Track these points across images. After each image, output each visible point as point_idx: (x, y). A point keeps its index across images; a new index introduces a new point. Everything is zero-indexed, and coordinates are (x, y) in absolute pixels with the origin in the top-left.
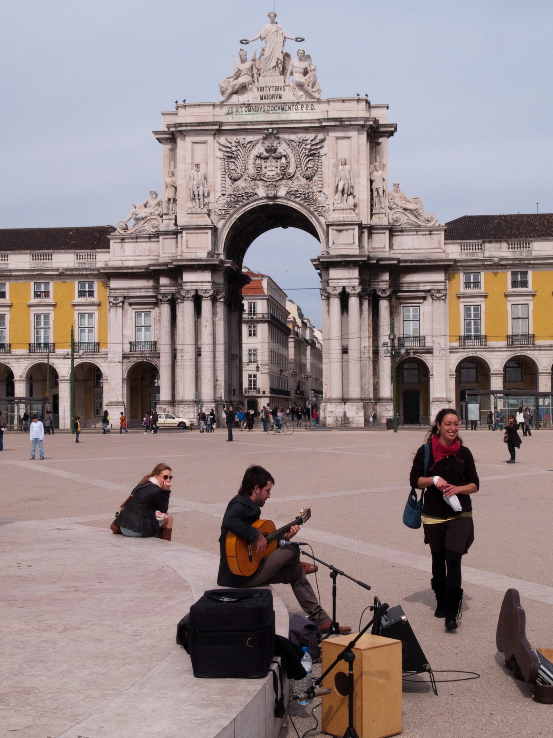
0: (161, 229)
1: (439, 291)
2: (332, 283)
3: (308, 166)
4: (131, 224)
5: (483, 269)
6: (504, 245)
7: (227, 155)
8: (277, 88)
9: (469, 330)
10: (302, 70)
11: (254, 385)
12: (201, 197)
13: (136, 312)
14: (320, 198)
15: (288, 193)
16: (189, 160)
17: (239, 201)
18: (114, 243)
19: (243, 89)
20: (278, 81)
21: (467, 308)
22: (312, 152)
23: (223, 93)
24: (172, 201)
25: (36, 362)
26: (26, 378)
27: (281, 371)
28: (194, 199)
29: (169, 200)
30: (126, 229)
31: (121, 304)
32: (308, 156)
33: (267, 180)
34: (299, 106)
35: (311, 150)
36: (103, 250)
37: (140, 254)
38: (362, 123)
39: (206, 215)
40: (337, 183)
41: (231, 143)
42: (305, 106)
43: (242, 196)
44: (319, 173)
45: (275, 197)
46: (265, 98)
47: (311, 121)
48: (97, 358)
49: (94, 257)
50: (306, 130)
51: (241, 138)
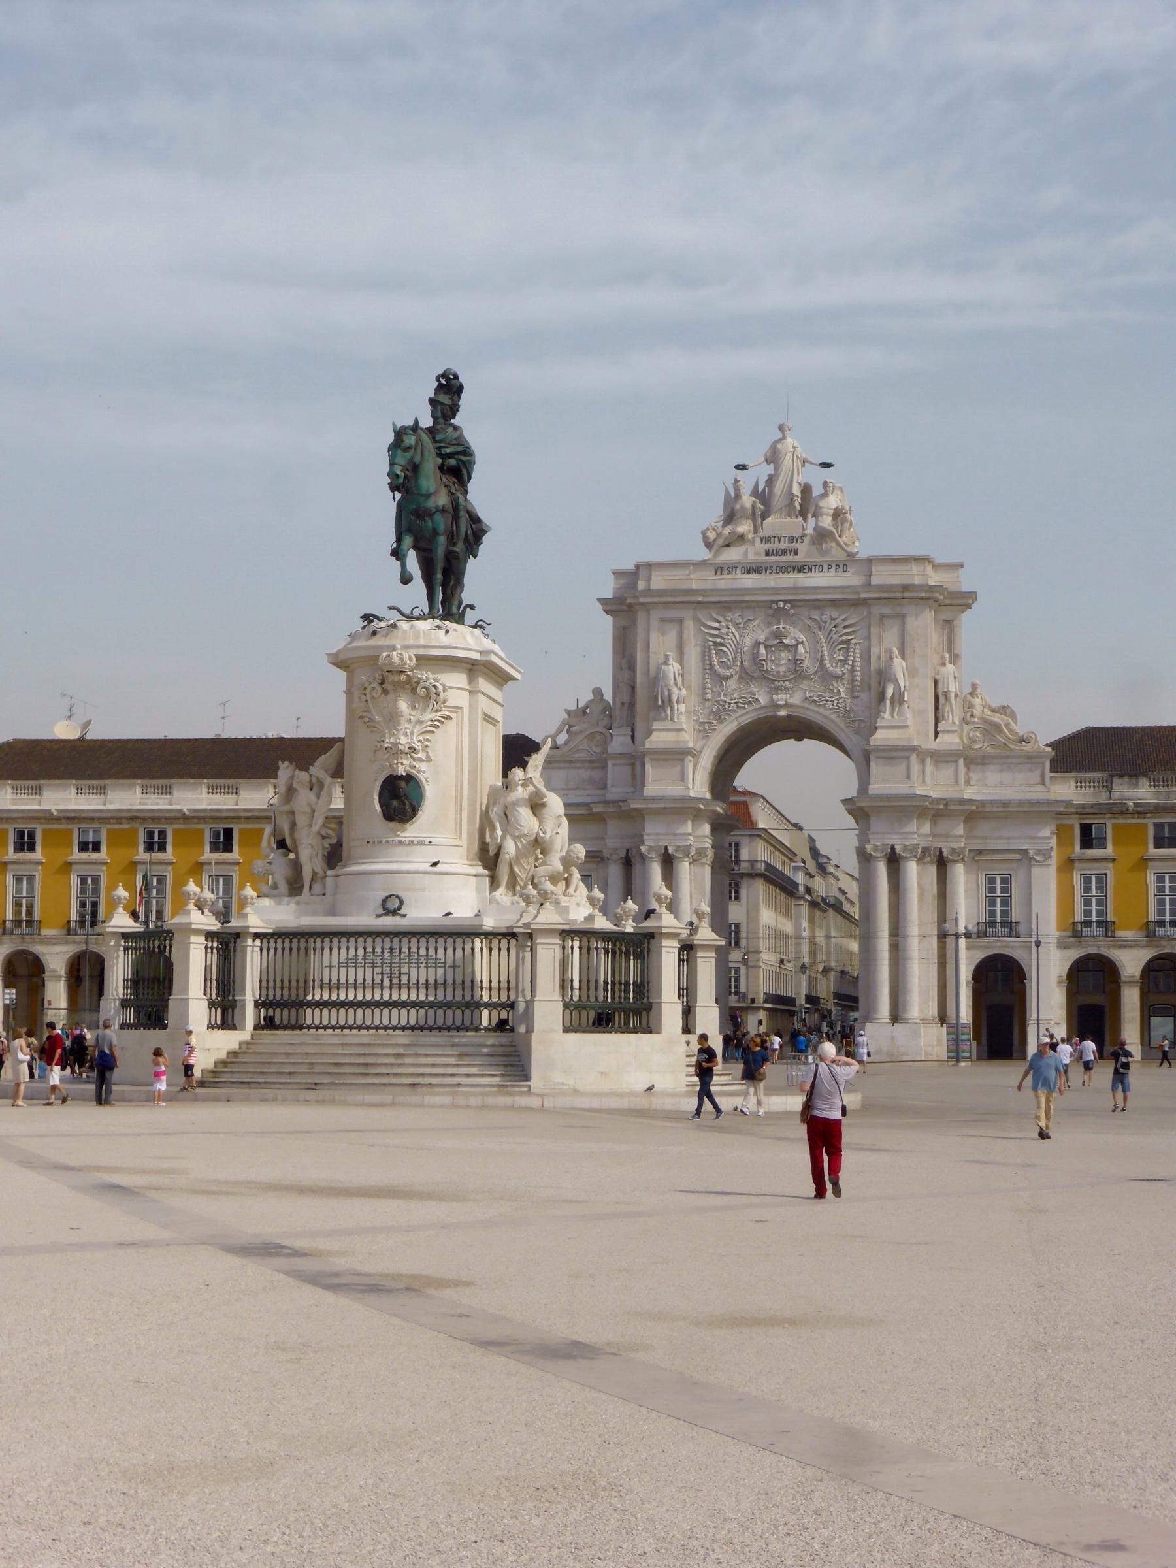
1: (1039, 852)
6: (1144, 782)
9: (1088, 913)
11: (737, 987)
21: (1087, 880)
22: (844, 638)
23: (709, 545)
27: (782, 961)
28: (663, 707)
29: (623, 704)
34: (825, 569)
41: (719, 622)
46: (773, 554)
47: (842, 589)
50: (834, 603)
51: (735, 616)
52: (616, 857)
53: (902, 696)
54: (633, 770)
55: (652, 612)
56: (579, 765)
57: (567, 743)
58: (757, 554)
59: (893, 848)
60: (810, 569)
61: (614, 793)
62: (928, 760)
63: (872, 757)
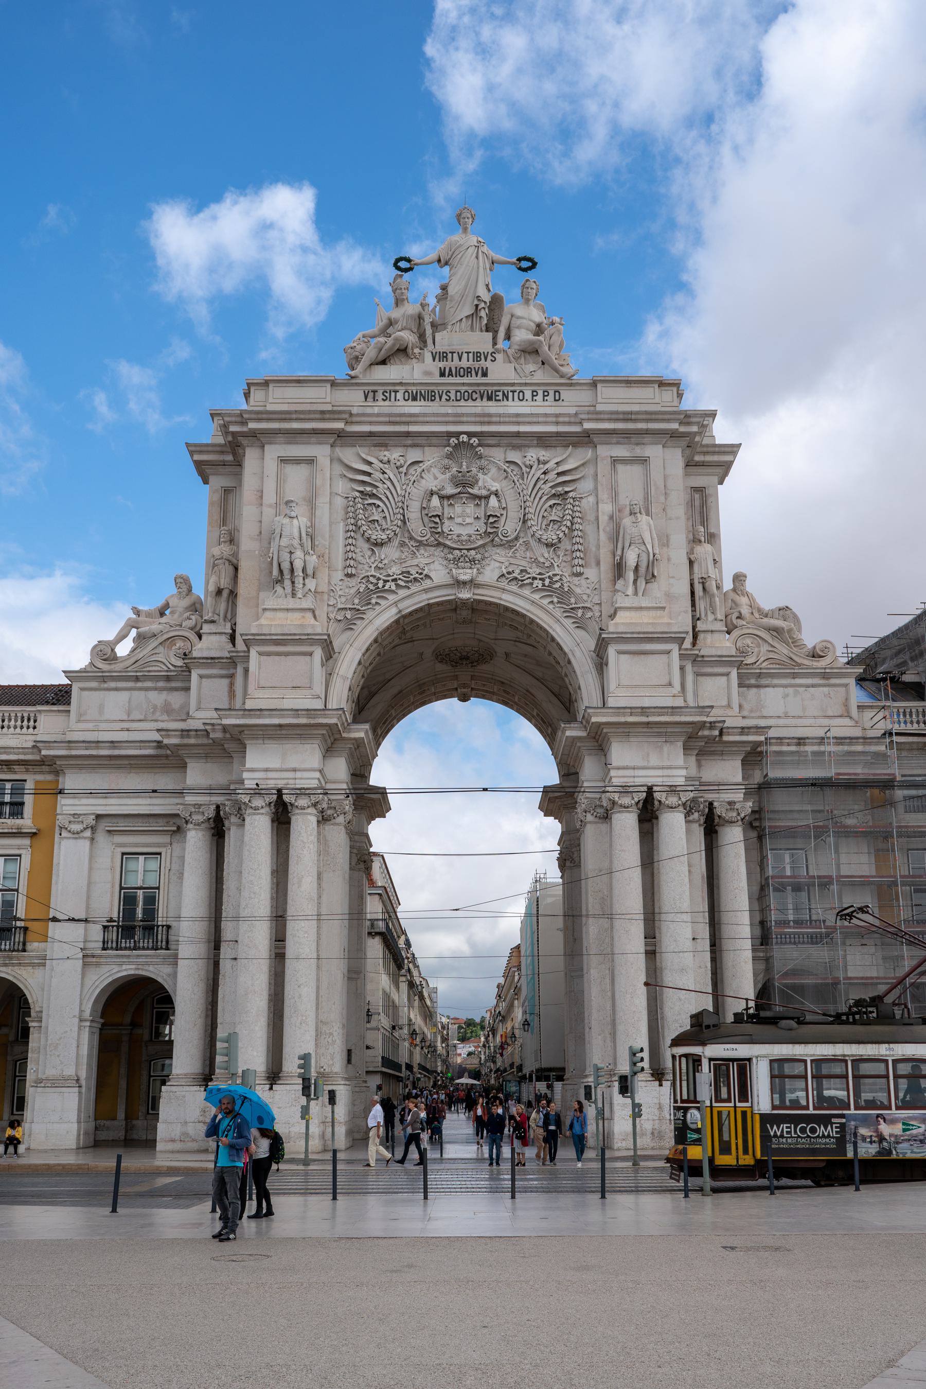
0: (195, 654)
2: (618, 778)
4: (124, 649)
7: (361, 489)
8: (477, 356)
10: (533, 326)
12: (299, 572)
13: (123, 854)
14: (578, 590)
15: (503, 575)
16: (270, 497)
17: (390, 591)
18: (82, 689)
19: (402, 352)
22: (560, 489)
23: (354, 361)
24: (225, 593)
29: (219, 592)
30: (111, 658)
31: (88, 833)
34: (528, 394)
36: (55, 708)
37: (142, 717)
38: (675, 426)
39: (309, 615)
40: (619, 552)
41: (370, 463)
42: (540, 393)
43: (395, 580)
44: (576, 533)
46: (450, 374)
47: (557, 419)
49: (32, 723)
50: (543, 440)
51: (394, 455)
52: (200, 818)
53: (651, 565)
54: (232, 685)
55: (267, 447)
56: (149, 684)
57: (133, 651)
58: (428, 373)
59: (650, 791)
60: (506, 397)
61: (201, 717)
62: (689, 668)
63: (611, 651)
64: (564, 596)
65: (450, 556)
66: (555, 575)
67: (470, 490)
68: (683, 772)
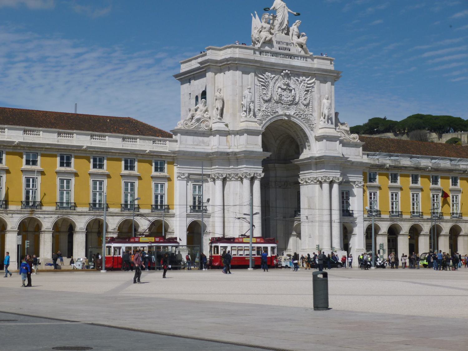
3: (306, 97)
5: (378, 170)
8: (287, 44)
14: (311, 119)
15: (294, 113)
17: (269, 116)
20: (286, 39)
22: (308, 89)
25: (125, 218)
26: (118, 230)
32: (306, 91)
33: (284, 103)
34: (299, 58)
35: (307, 87)
43: (270, 112)
45: (289, 116)
46: (281, 49)
48: (167, 217)
64: (308, 120)
65: (282, 106)
66: (306, 114)
67: (289, 88)
68: (340, 174)
